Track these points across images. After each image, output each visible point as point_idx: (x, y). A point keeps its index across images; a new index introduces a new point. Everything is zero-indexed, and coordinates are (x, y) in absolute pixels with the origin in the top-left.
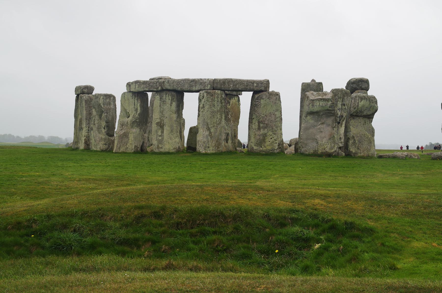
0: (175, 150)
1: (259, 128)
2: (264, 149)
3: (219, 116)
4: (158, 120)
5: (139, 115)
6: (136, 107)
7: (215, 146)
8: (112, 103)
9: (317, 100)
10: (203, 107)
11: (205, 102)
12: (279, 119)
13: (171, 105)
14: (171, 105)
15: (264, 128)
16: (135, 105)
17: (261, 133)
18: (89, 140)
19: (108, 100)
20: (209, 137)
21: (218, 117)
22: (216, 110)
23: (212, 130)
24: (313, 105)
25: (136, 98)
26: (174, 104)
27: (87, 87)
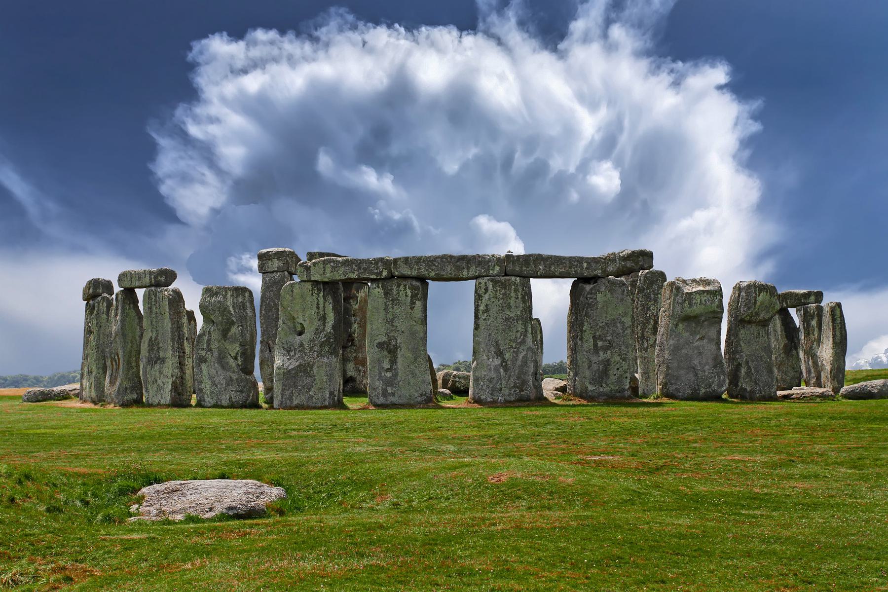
1: (596, 350)
2: (607, 389)
3: (520, 327)
4: (384, 339)
5: (334, 327)
6: (321, 312)
7: (515, 386)
8: (248, 304)
10: (487, 310)
11: (489, 299)
13: (412, 308)
14: (412, 308)
15: (605, 349)
16: (318, 308)
17: (600, 359)
18: (182, 384)
19: (240, 299)
20: (502, 370)
21: (520, 329)
22: (513, 315)
23: (508, 356)
24: (690, 304)
25: (322, 294)
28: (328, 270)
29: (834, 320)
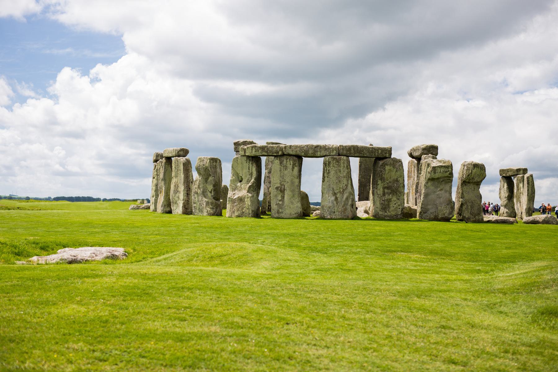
0: (297, 215)
2: (389, 214)
3: (345, 182)
4: (279, 185)
6: (251, 171)
9: (438, 167)
12: (402, 185)
13: (293, 170)
14: (293, 170)
18: (188, 204)
19: (215, 164)
20: (335, 203)
23: (338, 195)
24: (435, 173)
26: (296, 169)
27: (182, 150)
28: (254, 150)
29: (528, 183)
